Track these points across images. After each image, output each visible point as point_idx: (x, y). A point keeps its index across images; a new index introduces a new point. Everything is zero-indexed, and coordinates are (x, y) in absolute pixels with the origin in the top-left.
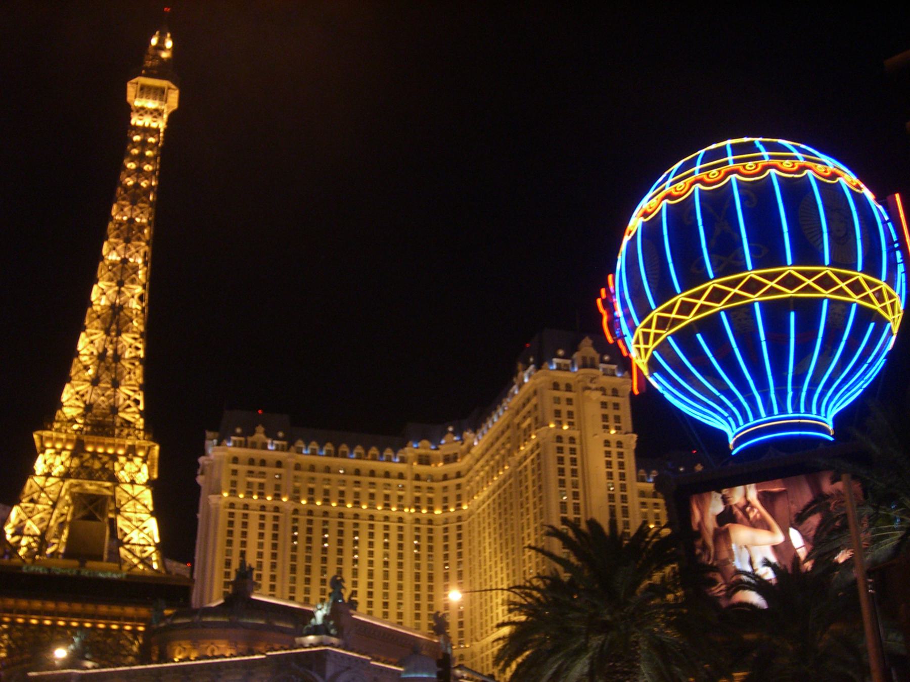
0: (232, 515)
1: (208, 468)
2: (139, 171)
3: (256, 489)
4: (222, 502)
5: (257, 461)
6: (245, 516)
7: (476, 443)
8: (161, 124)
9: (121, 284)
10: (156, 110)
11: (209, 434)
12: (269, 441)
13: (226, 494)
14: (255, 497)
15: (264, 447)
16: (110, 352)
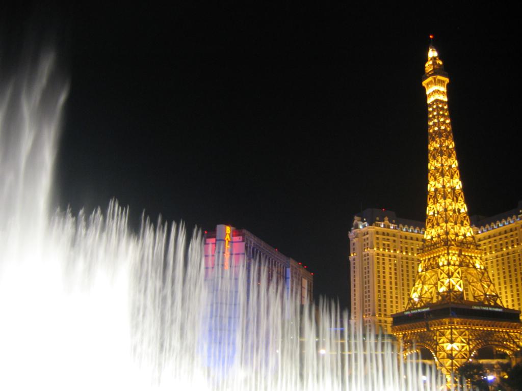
0: (378, 259)
1: (360, 235)
2: (444, 122)
3: (386, 247)
4: (374, 253)
5: (386, 234)
6: (384, 259)
7: (479, 232)
8: (445, 99)
9: (452, 177)
10: (444, 92)
11: (356, 218)
12: (390, 224)
13: (375, 249)
14: (387, 251)
15: (389, 227)
16: (457, 211)
